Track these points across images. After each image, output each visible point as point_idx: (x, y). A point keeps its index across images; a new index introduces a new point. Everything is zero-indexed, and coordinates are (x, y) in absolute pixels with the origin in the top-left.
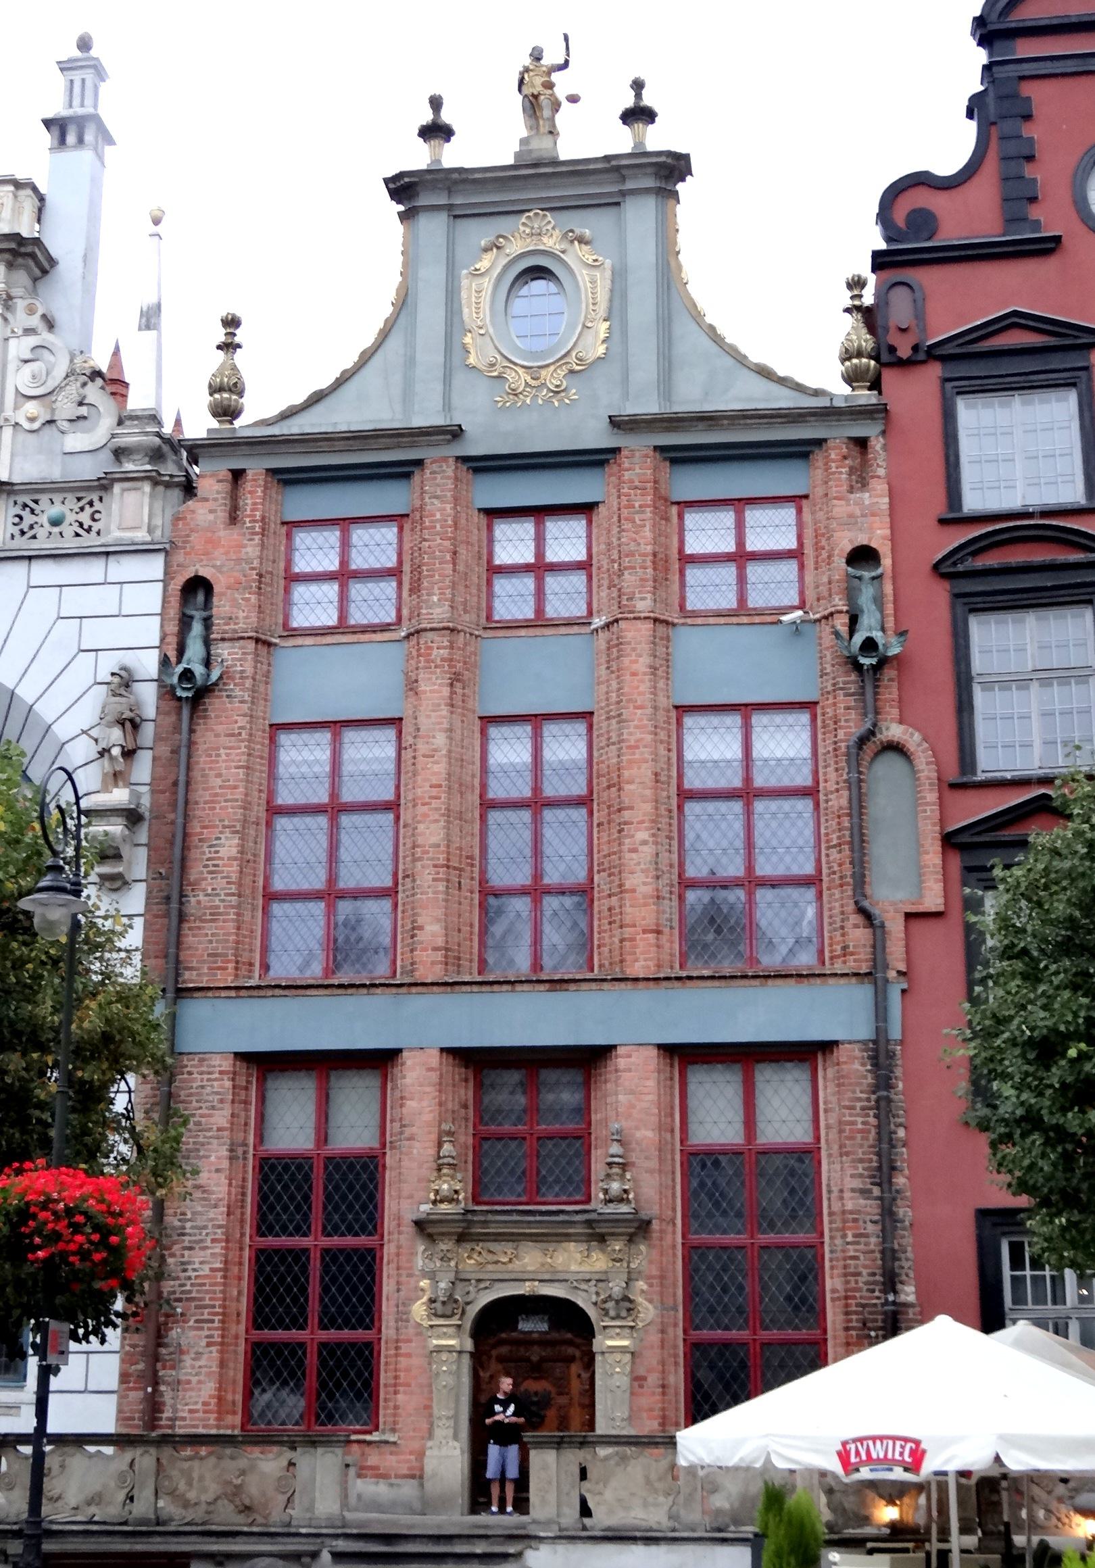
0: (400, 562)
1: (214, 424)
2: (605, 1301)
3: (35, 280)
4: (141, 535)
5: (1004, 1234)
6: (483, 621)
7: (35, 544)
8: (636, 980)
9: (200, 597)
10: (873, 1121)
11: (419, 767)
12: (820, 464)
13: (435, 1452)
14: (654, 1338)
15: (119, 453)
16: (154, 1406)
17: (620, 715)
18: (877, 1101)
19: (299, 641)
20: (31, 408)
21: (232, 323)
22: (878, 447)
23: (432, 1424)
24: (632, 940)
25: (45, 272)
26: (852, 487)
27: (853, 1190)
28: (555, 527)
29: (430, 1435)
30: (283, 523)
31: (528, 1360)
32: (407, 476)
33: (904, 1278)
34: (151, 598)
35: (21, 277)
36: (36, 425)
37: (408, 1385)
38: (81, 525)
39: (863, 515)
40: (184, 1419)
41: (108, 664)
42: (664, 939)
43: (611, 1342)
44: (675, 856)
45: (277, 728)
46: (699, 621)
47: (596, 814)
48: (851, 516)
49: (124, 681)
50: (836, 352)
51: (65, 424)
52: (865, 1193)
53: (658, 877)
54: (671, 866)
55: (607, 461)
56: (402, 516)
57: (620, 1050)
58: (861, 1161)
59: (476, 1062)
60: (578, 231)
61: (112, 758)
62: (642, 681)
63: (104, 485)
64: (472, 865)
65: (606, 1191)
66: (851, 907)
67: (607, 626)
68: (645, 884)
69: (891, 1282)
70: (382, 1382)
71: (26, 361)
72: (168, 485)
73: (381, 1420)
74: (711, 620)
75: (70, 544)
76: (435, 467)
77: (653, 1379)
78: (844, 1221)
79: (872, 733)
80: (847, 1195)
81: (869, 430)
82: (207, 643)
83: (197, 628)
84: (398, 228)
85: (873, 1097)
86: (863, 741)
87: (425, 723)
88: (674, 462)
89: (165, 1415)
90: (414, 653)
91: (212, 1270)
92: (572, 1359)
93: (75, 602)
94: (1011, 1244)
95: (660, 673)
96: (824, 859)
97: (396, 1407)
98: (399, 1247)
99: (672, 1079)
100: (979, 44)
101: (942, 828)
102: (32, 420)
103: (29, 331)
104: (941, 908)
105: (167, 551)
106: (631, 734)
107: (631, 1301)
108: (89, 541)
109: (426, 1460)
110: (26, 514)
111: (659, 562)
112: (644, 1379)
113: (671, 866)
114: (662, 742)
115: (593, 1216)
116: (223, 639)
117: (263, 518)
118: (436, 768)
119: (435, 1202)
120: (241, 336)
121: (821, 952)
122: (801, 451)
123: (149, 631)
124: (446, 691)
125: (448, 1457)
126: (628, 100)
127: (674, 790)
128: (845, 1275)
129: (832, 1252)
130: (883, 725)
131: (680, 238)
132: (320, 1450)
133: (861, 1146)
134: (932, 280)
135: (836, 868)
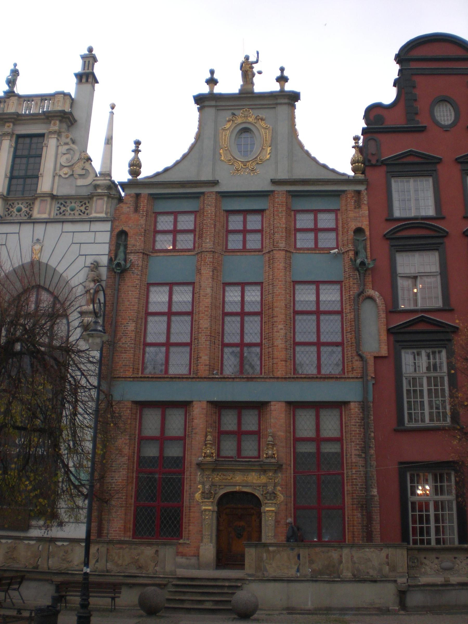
0: (195, 227)
1: (130, 177)
2: (265, 494)
3: (69, 127)
4: (103, 215)
6: (224, 249)
7: (64, 217)
8: (278, 378)
9: (123, 237)
10: (362, 430)
11: (201, 300)
12: (344, 199)
15: (96, 187)
17: (273, 284)
18: (364, 423)
19: (158, 254)
20: (65, 170)
21: (138, 143)
22: (365, 194)
23: (202, 537)
25: (72, 124)
26: (355, 207)
28: (250, 218)
30: (153, 213)
32: (198, 198)
33: (373, 486)
34: (106, 237)
35: (64, 126)
36: (67, 176)
37: (194, 523)
38: (81, 211)
39: (360, 218)
40: (112, 533)
41: (90, 260)
42: (288, 363)
43: (268, 508)
44: (292, 334)
45: (149, 285)
46: (301, 252)
47: (264, 319)
49: (95, 266)
50: (349, 161)
51: (77, 176)
52: (359, 456)
53: (286, 342)
54: (291, 338)
55: (270, 195)
56: (196, 211)
57: (272, 403)
58: (358, 444)
59: (219, 406)
60: (261, 116)
61: (90, 293)
63: (90, 198)
64: (219, 336)
65: (267, 454)
66: (355, 354)
67: (269, 252)
70: (184, 521)
71: (64, 154)
72: (113, 198)
73: (184, 535)
74: (306, 252)
75: (77, 217)
78: (352, 466)
79: (362, 292)
80: (353, 456)
81: (362, 188)
82: (125, 253)
83: (122, 249)
84: (197, 114)
85: (363, 422)
86: (359, 295)
87: (203, 284)
88: (293, 196)
89: (105, 532)
90: (200, 260)
93: (79, 238)
95: (287, 269)
96: (345, 336)
97: (189, 531)
98: (190, 473)
99: (290, 414)
100: (397, 63)
101: (387, 327)
102: (66, 174)
103: (67, 144)
104: (386, 355)
105: (113, 220)
106: (277, 290)
107: (275, 494)
108: (84, 217)
110: (62, 206)
111: (287, 230)
112: (280, 522)
114: (288, 293)
115: (262, 463)
116: (131, 253)
117: (147, 211)
118: (207, 300)
119: (204, 457)
120: (141, 147)
121: (343, 369)
122: (337, 194)
123: (105, 249)
124: (211, 273)
126: (279, 74)
127: (292, 311)
128: (352, 485)
130: (367, 290)
131: (296, 120)
133: (358, 439)
134: (383, 138)
135: (350, 340)
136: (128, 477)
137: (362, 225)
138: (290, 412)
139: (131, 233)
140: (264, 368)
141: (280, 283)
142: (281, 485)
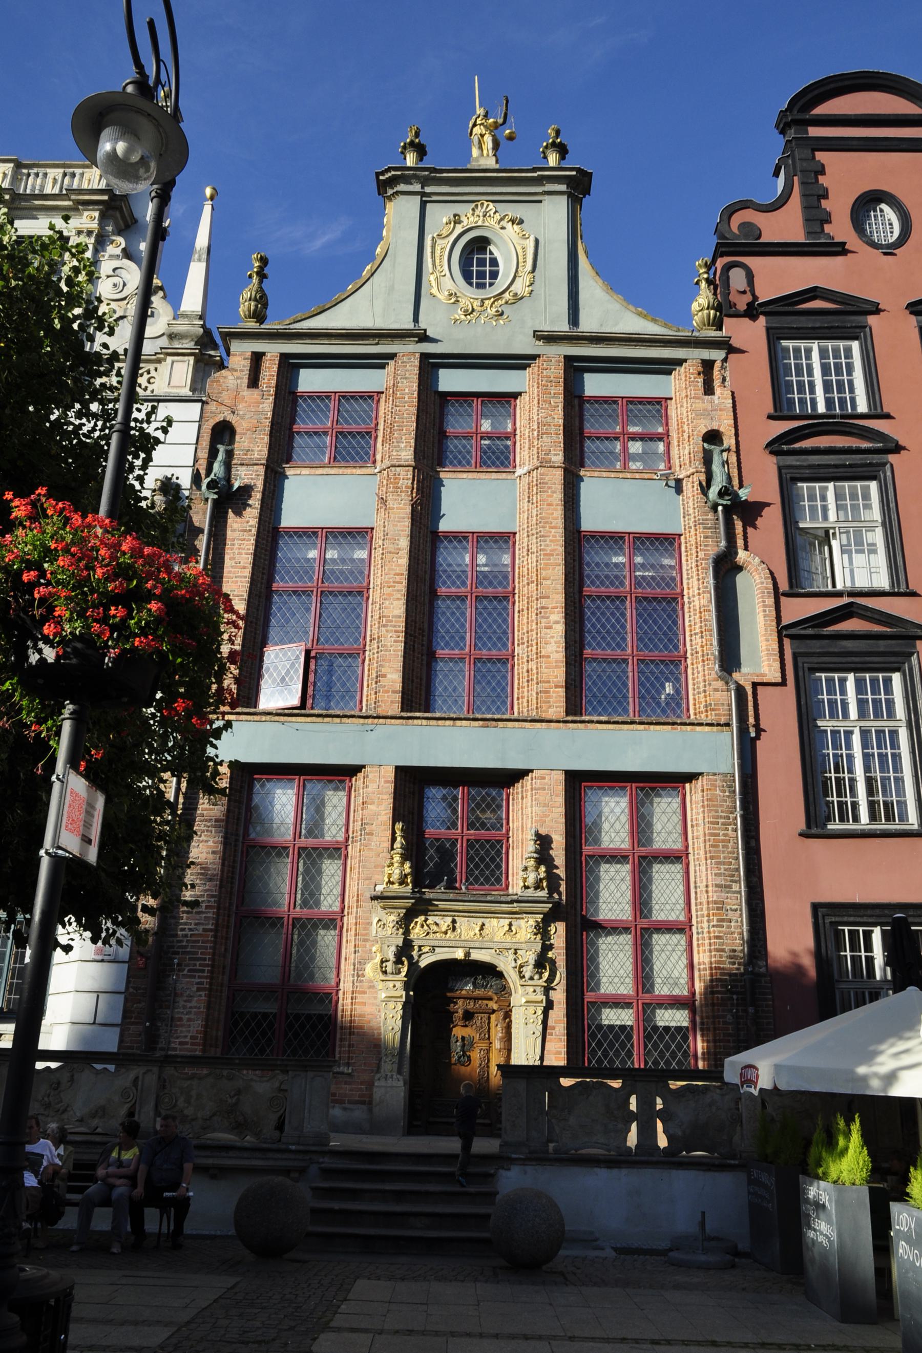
13: (382, 1083)
15: (172, 337)
16: (152, 1038)
23: (380, 1060)
24: (547, 692)
27: (717, 886)
29: (378, 1071)
40: (175, 1049)
48: (705, 410)
55: (529, 366)
62: (556, 510)
64: (423, 636)
68: (557, 652)
76: (405, 359)
81: (717, 355)
89: (160, 1046)
91: (204, 930)
106: (547, 545)
109: (375, 1090)
113: (575, 642)
116: (242, 464)
125: (392, 1087)
132: (311, 1074)
136: (217, 925)
137: (720, 426)
139: (240, 425)
140: (518, 704)
141: (553, 531)
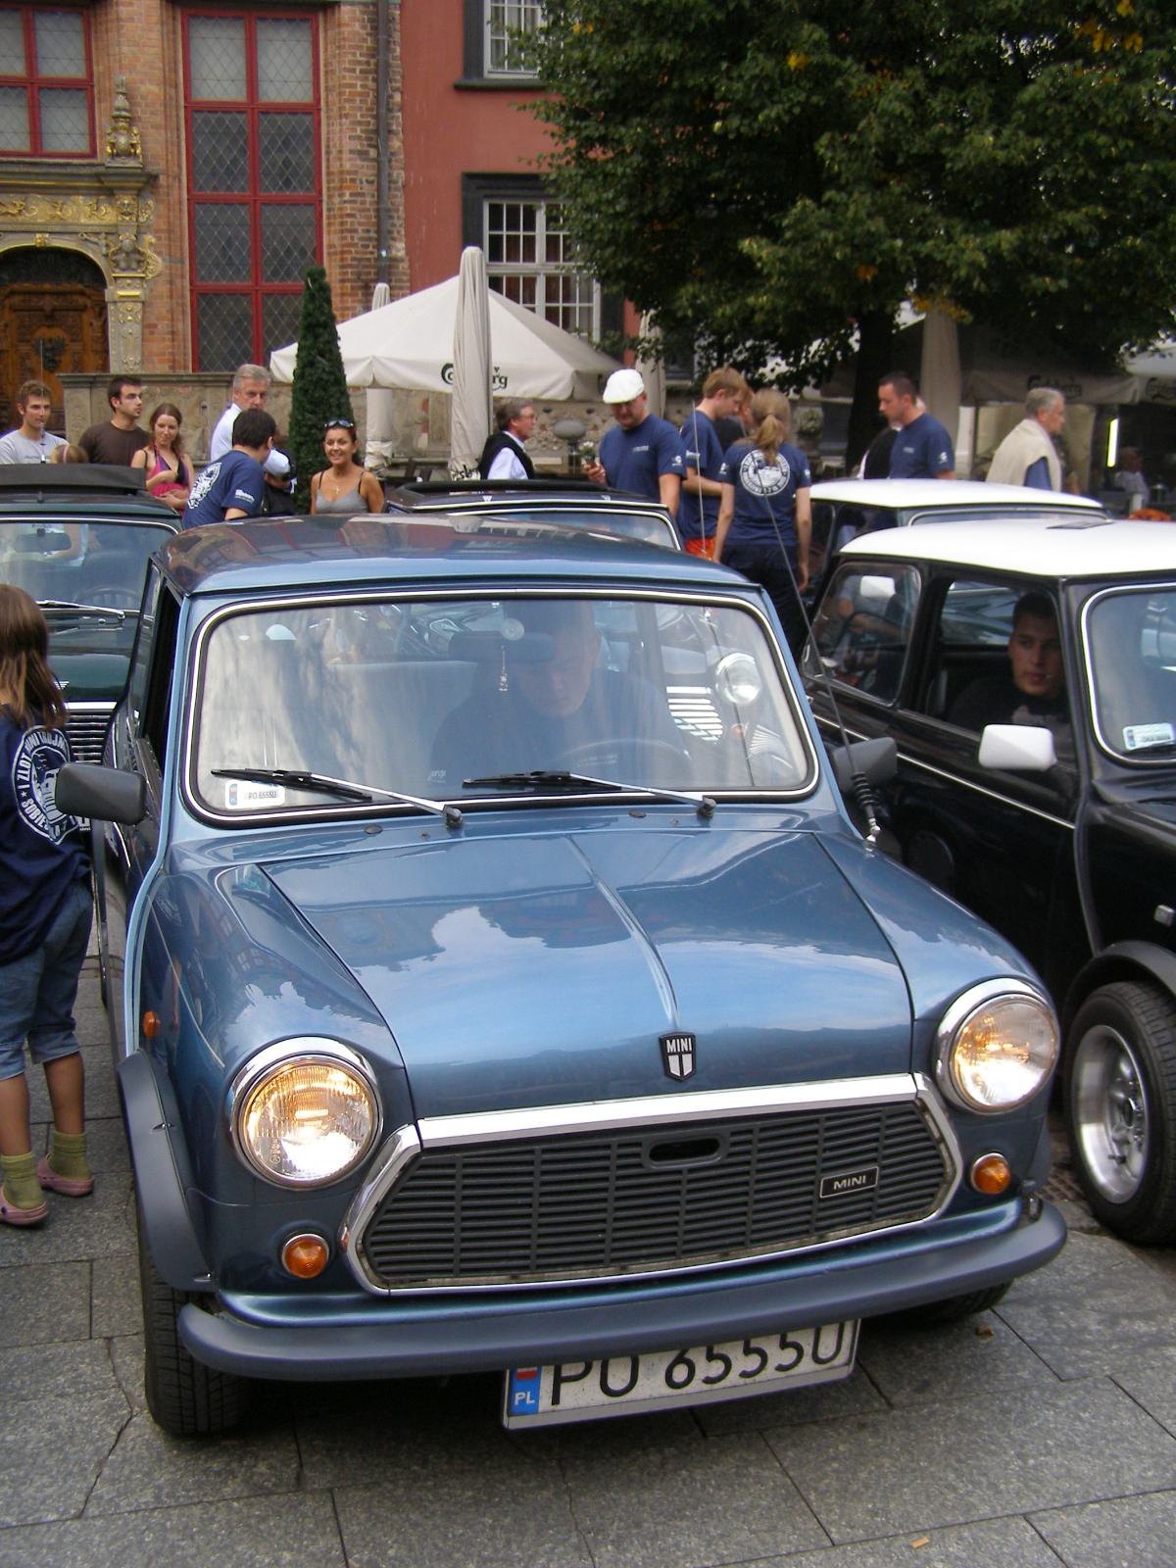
2: (115, 254)
5: (486, 197)
10: (370, 83)
14: (163, 288)
18: (377, 65)
27: (351, 152)
31: (42, 310)
43: (122, 292)
52: (363, 154)
58: (360, 123)
65: (113, 145)
69: (382, 238)
77: (163, 326)
78: (342, 181)
80: (346, 156)
85: (372, 61)
92: (84, 309)
94: (492, 207)
99: (174, 32)
107: (139, 252)
112: (155, 326)
115: (101, 169)
128: (342, 232)
129: (329, 210)
133: (360, 109)
138: (174, 26)
142: (157, 231)
